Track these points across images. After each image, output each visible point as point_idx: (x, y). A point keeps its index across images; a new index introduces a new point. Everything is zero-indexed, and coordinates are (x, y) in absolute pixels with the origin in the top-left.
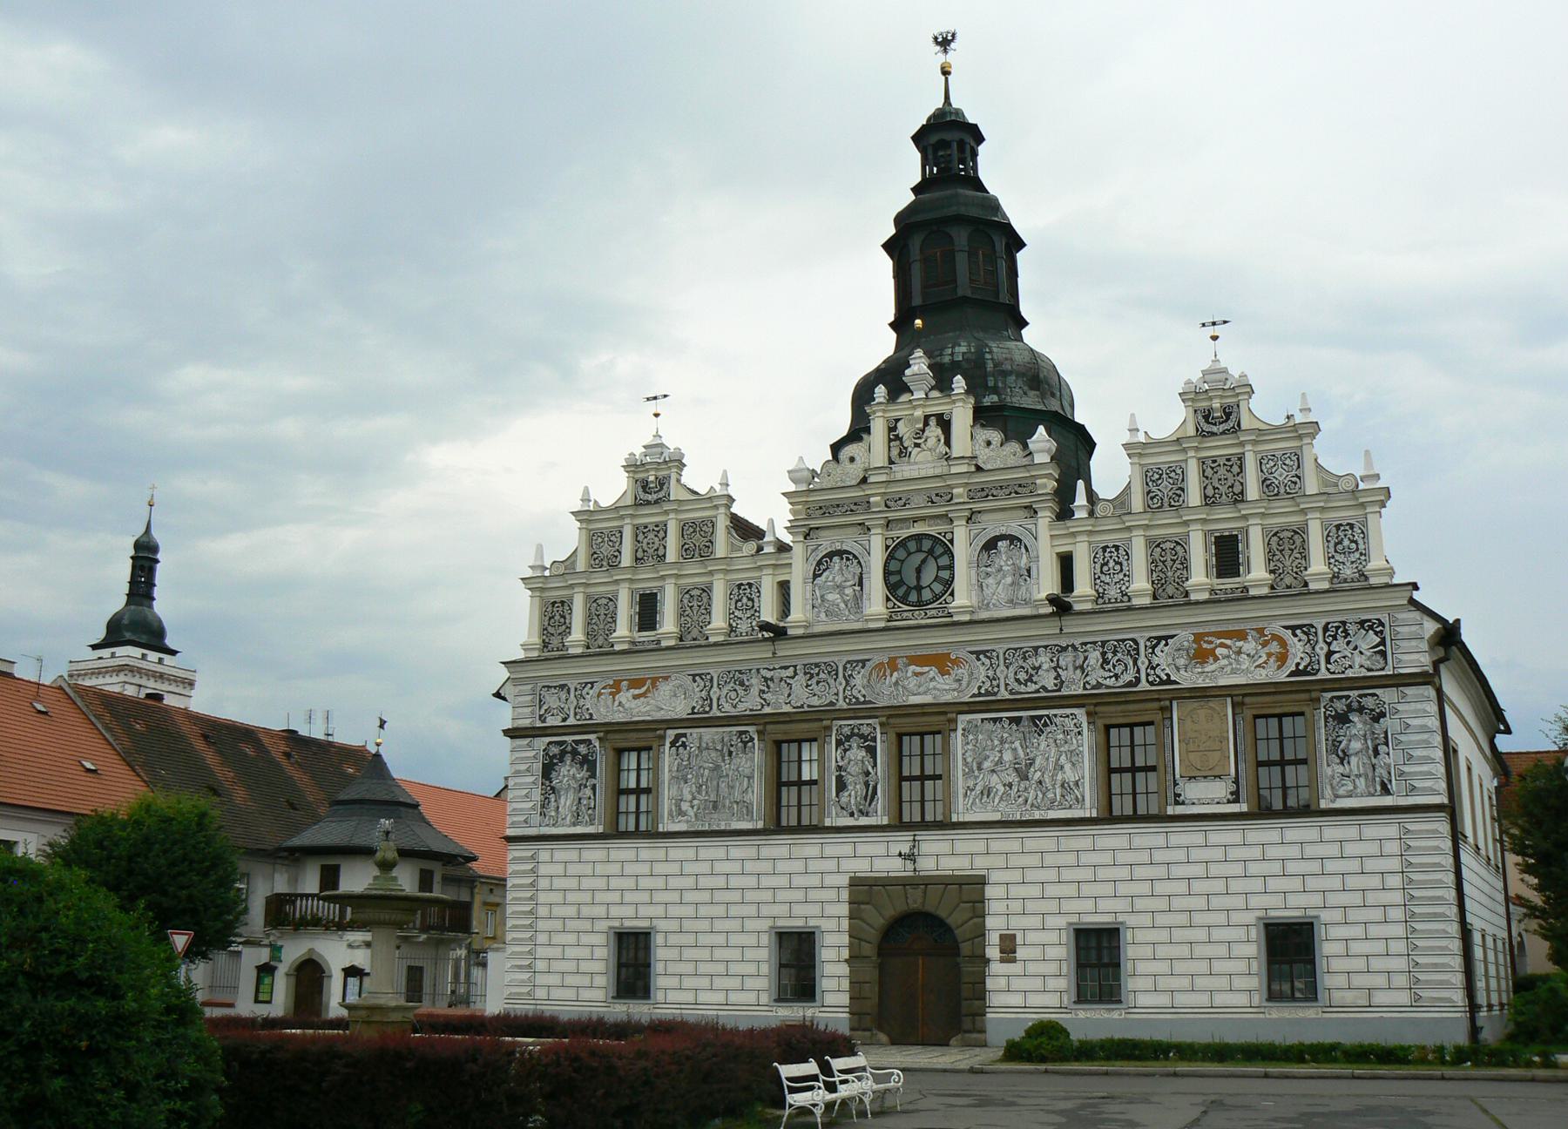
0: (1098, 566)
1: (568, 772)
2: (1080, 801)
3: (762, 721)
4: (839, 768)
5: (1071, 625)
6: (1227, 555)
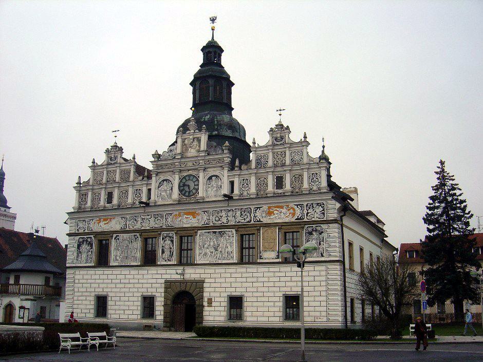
0: (241, 185)
1: (85, 247)
2: (232, 258)
3: (141, 232)
4: (163, 246)
5: (232, 203)
6: (279, 182)
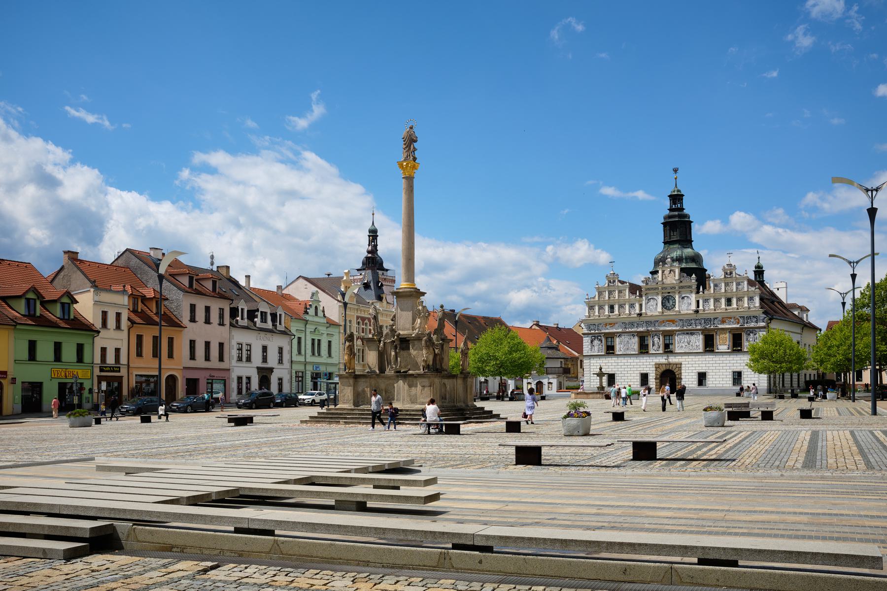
1: (596, 342)
